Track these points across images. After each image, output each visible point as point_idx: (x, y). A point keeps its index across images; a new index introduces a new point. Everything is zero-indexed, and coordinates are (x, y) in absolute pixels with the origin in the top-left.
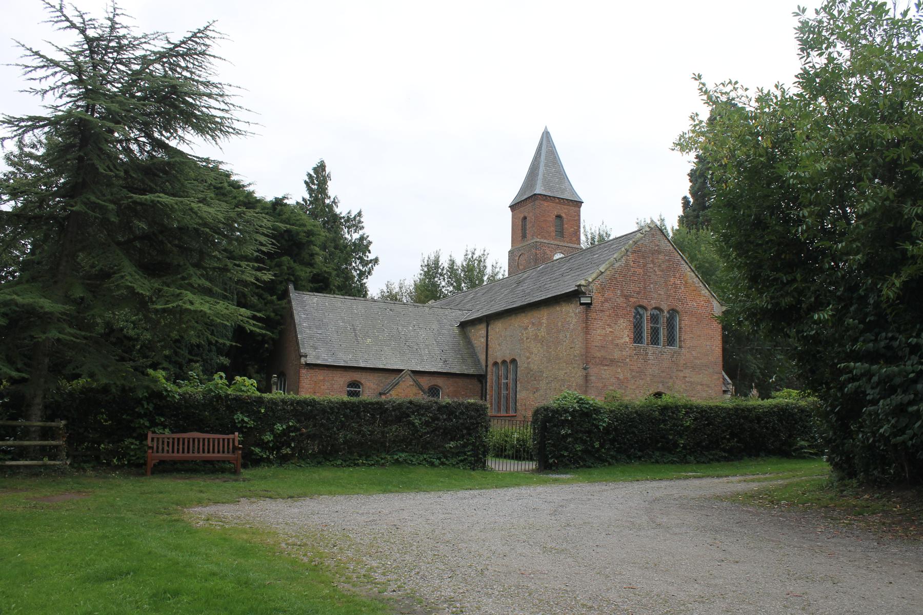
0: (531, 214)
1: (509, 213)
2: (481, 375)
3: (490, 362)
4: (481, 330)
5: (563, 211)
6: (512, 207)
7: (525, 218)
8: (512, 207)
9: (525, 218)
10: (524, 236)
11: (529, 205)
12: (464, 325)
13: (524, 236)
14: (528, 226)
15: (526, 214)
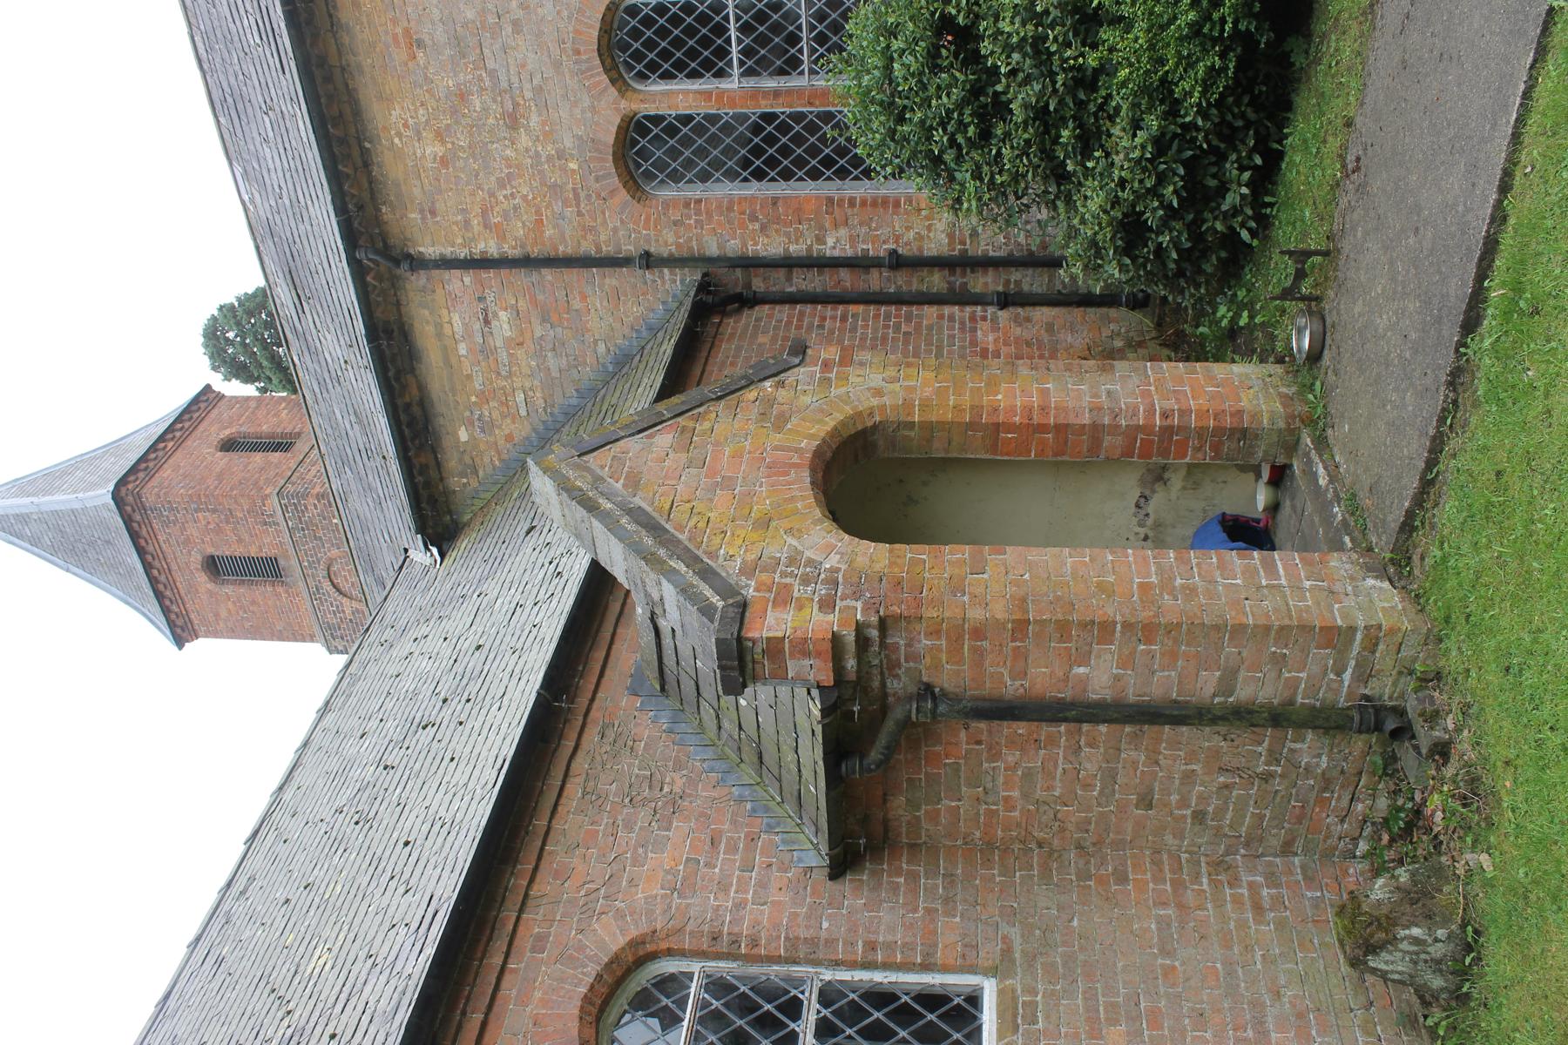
0: (192, 531)
1: (202, 648)
2: (703, 287)
3: (621, 223)
4: (449, 318)
5: (214, 429)
6: (181, 632)
7: (213, 566)
8: (181, 632)
9: (213, 566)
10: (267, 569)
11: (166, 539)
12: (438, 520)
13: (267, 569)
14: (229, 548)
15: (196, 559)
